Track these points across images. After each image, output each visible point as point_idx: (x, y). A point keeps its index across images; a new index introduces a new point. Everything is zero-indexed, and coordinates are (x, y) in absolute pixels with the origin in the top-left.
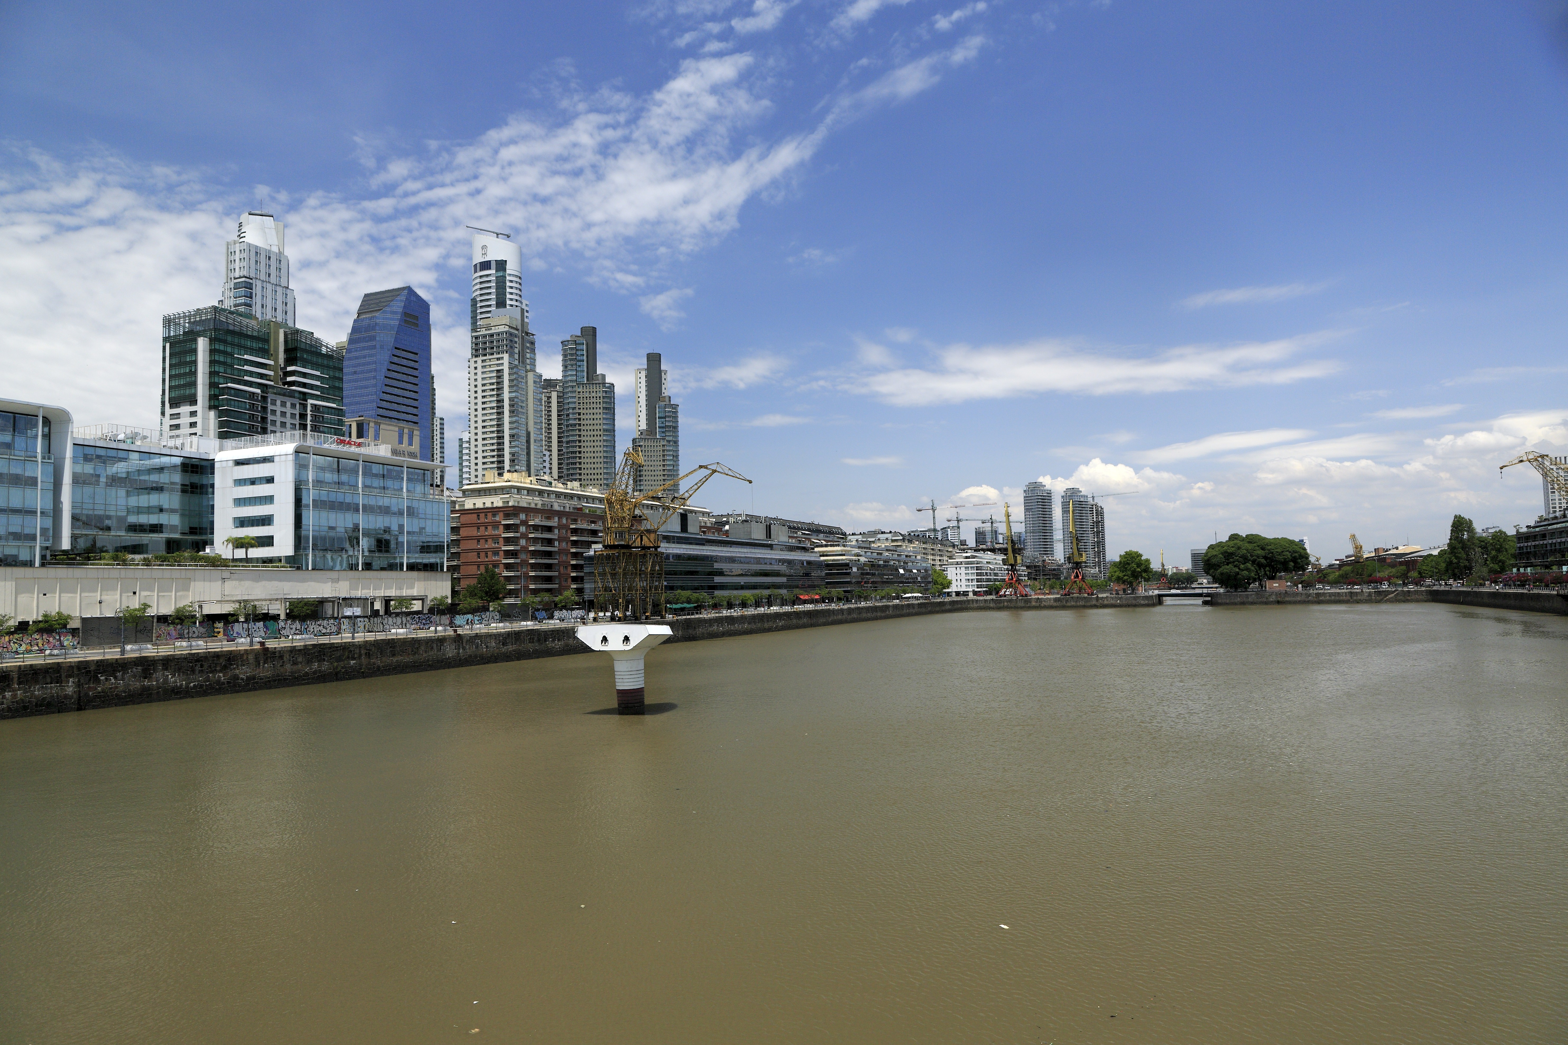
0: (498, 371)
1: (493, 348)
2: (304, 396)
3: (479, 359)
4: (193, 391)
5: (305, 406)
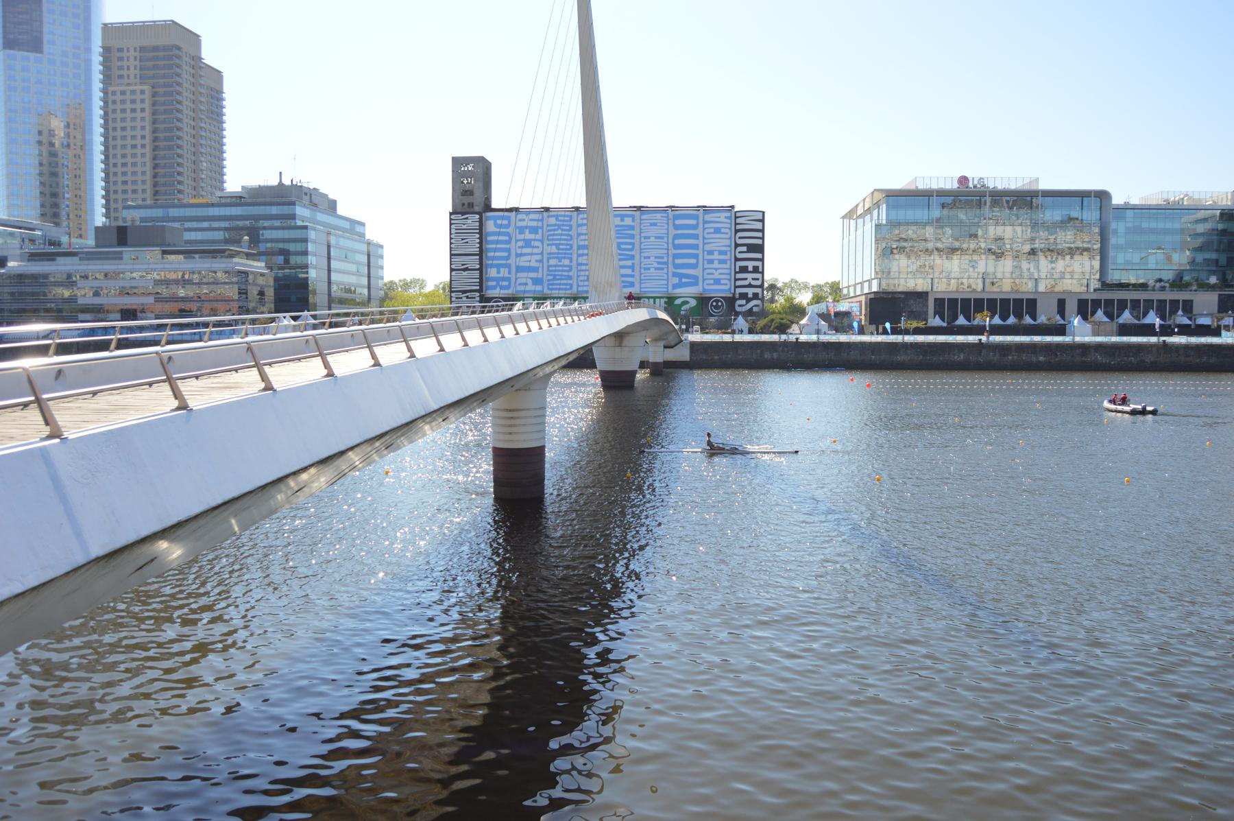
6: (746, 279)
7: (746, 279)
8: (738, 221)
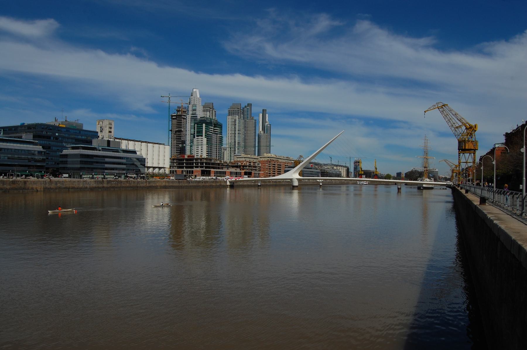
0: (235, 120)
1: (233, 114)
2: (217, 134)
3: (230, 116)
4: (202, 134)
5: (217, 136)
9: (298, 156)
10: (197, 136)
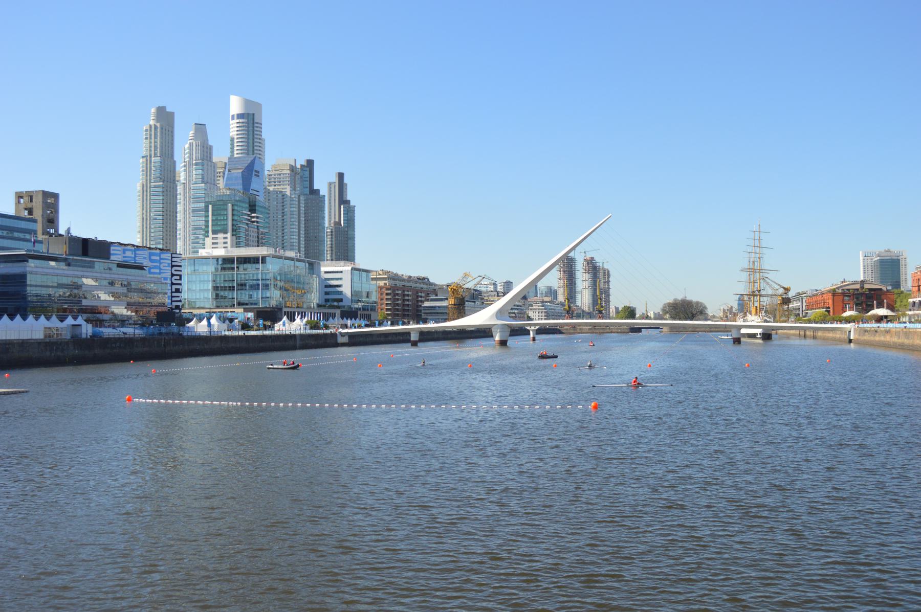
6: (179, 297)
7: (179, 297)
8: (173, 259)
9: (461, 275)
10: (214, 232)
